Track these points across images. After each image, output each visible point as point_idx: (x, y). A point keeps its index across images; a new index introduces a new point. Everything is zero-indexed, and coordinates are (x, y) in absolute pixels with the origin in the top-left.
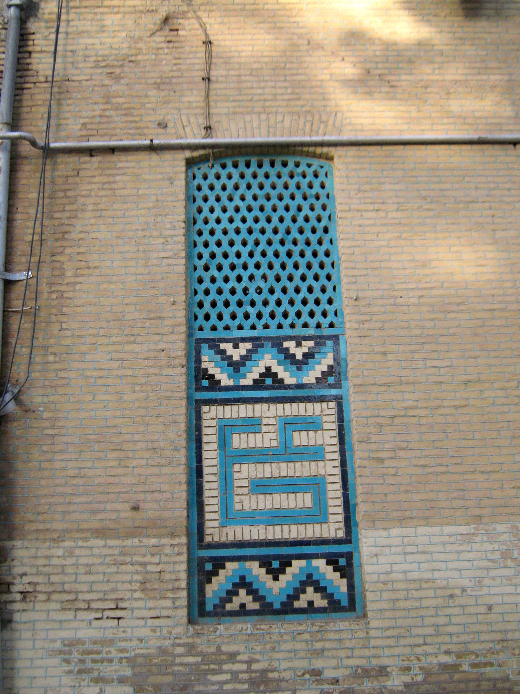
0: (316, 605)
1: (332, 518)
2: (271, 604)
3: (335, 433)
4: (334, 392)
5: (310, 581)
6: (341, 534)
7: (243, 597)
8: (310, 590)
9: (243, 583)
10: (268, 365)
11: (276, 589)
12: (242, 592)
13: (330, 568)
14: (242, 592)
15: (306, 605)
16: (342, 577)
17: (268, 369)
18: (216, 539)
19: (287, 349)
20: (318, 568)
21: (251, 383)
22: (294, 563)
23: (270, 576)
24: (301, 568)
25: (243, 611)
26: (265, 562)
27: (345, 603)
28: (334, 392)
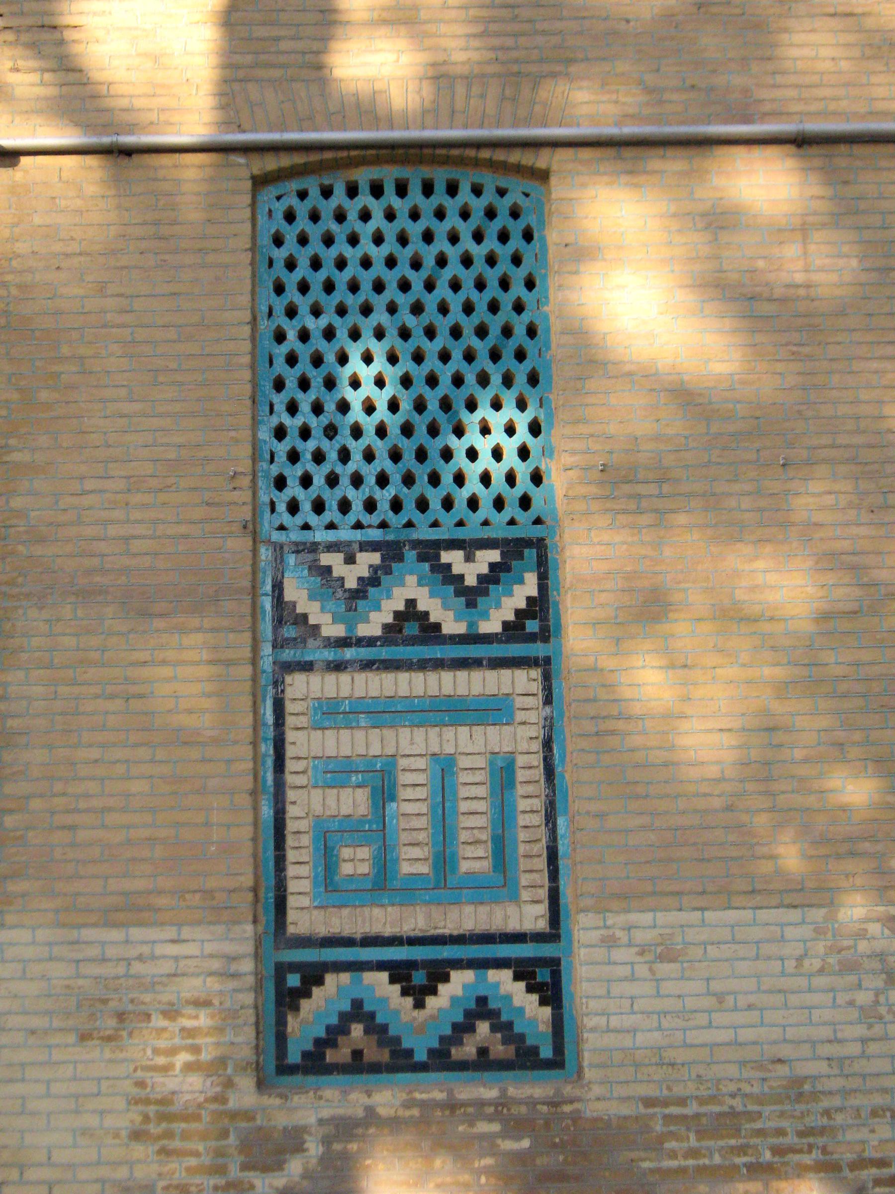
0: (492, 1056)
2: (410, 1053)
4: (538, 649)
5: (481, 1009)
10: (411, 596)
13: (522, 985)
16: (543, 1002)
17: (411, 603)
19: (449, 566)
20: (497, 985)
23: (409, 1001)
26: (399, 972)
27: (546, 1052)
28: (538, 649)
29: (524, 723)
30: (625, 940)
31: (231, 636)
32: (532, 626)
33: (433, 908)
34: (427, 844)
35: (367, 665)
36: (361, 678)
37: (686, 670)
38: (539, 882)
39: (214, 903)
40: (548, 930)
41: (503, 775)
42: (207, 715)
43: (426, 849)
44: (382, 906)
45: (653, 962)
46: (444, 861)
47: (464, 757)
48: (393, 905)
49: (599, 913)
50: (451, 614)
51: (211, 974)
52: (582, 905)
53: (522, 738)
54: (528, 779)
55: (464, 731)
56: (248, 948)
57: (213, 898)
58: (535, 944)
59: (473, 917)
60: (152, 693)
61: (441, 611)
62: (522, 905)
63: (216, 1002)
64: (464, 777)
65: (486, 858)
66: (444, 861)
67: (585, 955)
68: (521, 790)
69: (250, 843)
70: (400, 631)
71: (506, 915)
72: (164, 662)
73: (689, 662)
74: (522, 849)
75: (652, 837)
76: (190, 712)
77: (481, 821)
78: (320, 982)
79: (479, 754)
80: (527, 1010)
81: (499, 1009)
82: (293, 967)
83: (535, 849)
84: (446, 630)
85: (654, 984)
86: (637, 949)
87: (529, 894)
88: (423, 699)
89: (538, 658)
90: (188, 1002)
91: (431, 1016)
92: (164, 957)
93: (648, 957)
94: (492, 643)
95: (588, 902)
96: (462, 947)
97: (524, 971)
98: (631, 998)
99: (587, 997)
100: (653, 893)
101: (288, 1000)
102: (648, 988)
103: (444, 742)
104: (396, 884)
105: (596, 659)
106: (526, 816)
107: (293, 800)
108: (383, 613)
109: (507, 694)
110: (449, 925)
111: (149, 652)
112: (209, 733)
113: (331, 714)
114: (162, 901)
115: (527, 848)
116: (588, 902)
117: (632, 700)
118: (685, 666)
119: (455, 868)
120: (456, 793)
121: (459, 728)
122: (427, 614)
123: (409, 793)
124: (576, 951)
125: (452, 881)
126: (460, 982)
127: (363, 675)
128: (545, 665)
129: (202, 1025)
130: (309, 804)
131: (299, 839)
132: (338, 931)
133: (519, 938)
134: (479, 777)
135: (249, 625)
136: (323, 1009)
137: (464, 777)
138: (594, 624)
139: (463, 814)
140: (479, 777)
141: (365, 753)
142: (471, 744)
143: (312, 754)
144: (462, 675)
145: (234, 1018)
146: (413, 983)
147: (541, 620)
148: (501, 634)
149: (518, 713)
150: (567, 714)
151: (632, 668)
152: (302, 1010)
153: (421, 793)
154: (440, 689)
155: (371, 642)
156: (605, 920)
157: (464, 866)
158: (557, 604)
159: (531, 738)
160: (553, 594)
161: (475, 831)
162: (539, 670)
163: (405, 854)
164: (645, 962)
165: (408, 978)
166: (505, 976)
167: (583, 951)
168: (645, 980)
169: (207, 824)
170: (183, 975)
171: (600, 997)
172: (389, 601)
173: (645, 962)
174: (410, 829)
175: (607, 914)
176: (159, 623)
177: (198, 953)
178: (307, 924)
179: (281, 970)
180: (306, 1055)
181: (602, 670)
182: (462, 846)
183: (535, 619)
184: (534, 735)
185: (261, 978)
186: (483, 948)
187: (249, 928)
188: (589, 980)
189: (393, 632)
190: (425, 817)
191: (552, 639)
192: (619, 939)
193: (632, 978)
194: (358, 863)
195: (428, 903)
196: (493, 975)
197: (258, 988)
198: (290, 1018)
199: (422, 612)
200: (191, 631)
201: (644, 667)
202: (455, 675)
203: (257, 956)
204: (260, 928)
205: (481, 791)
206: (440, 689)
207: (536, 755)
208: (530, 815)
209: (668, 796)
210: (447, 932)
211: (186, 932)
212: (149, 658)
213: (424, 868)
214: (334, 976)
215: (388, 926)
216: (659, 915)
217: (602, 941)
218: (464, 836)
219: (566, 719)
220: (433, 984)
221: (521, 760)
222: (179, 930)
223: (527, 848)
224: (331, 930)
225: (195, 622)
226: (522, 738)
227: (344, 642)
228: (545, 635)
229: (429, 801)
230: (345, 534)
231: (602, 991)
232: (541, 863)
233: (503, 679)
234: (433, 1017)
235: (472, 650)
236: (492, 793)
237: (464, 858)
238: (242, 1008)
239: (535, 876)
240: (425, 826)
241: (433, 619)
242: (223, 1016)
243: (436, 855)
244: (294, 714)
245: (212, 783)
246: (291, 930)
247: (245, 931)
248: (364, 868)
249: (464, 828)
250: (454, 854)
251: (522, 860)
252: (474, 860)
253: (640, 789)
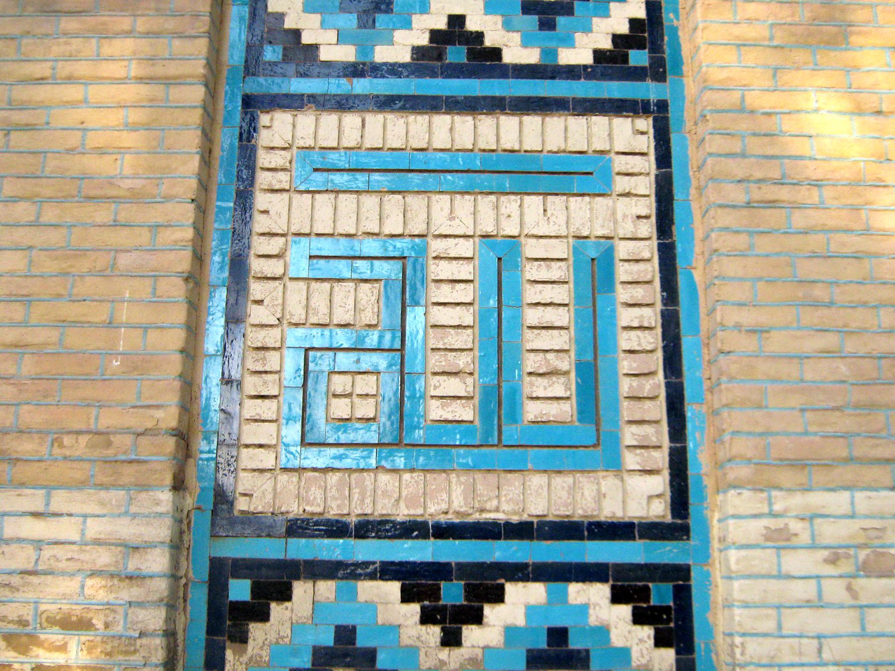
3: (648, 206)
13: (625, 611)
16: (661, 641)
20: (584, 609)
21: (406, 57)
22: (512, 590)
23: (434, 632)
24: (530, 610)
26: (418, 583)
28: (650, 91)
29: (628, 195)
30: (805, 538)
31: (177, 43)
32: (638, 58)
33: (479, 476)
34: (471, 374)
35: (386, 103)
36: (375, 120)
37: (880, 117)
38: (654, 440)
39: (110, 452)
40: (669, 519)
41: (596, 269)
42: (128, 157)
43: (470, 380)
44: (395, 471)
45: (854, 577)
46: (498, 401)
47: (533, 241)
48: (412, 470)
49: (761, 490)
50: (516, 37)
51: (93, 574)
52: (731, 476)
53: (625, 216)
54: (635, 278)
55: (533, 203)
56: (162, 531)
57: (109, 444)
58: (648, 541)
59: (545, 493)
60: (48, 123)
61: (503, 32)
62: (626, 476)
63: (98, 623)
64: (533, 272)
65: (568, 398)
66: (498, 401)
67: (738, 562)
68: (623, 294)
69: (177, 358)
70: (440, 57)
71: (599, 491)
72: (70, 79)
73: (884, 109)
74: (626, 386)
75: (843, 369)
76: (101, 151)
77: (558, 340)
78: (285, 595)
79: (557, 237)
80: (635, 654)
81: (587, 651)
83: (648, 387)
84: (508, 58)
85: (854, 614)
86: (826, 553)
87: (638, 459)
88: (472, 154)
89: (649, 101)
90: (52, 621)
91: (470, 659)
92: (19, 540)
93: (846, 567)
94: (579, 78)
95: (742, 472)
96: (525, 543)
97: (628, 587)
98: (819, 637)
99: (743, 635)
100: (850, 460)
102: (846, 621)
103: (502, 219)
104: (419, 435)
105: (743, 97)
106: (633, 334)
107: (258, 298)
108: (414, 31)
109: (602, 152)
110: (505, 507)
111: (49, 64)
112: (128, 183)
113: (327, 169)
114: (26, 447)
115: (635, 384)
116: (742, 472)
117: (801, 158)
118: (879, 113)
119: (514, 418)
120: (519, 295)
121: (527, 198)
122: (480, 36)
123: (445, 293)
124: (716, 554)
125: (511, 433)
126: (521, 601)
127: (380, 117)
128: (659, 111)
129: (70, 662)
130: (283, 304)
131: (264, 359)
132: (319, 510)
134: (556, 272)
135: (206, 28)
136: (287, 640)
137: (533, 272)
138: (739, 46)
139: (530, 328)
140: (556, 272)
141: (376, 231)
142: (544, 222)
143: (294, 229)
144: (532, 122)
145: (126, 653)
146: (441, 603)
147: (652, 51)
148: (591, 66)
149: (618, 178)
150: (694, 183)
151: (798, 111)
152: (250, 641)
153: (464, 293)
154: (498, 141)
155: (394, 70)
156: (770, 504)
157: (532, 411)
158: (675, 30)
159: (639, 217)
160: (668, 17)
161: (550, 356)
162: (650, 121)
163: (435, 387)
164: (841, 577)
165: (434, 593)
166: (597, 594)
167: (733, 555)
168: (842, 607)
169: (111, 324)
170: (45, 573)
171: (765, 635)
172: (425, 16)
173: (841, 577)
174: (446, 349)
175: (774, 493)
176: (70, 24)
177: (76, 537)
178: (269, 497)
179: (220, 572)
181: (752, 112)
182: (527, 379)
183: (644, 48)
184: (644, 213)
185: (186, 585)
186: (562, 547)
187: (165, 497)
188: (746, 605)
189: (428, 59)
190: (469, 331)
191: (669, 78)
192: (796, 535)
193: (818, 604)
194: (356, 400)
195: (468, 469)
196: (576, 592)
197: (174, 603)
198: (229, 654)
199: (471, 33)
200: (117, 35)
201: (816, 111)
202: (521, 123)
203: (177, 546)
204: (189, 502)
205: (560, 294)
206: (498, 141)
207: (647, 243)
208: (638, 333)
209: (864, 304)
210: (500, 517)
211: (60, 500)
212: (48, 73)
213: (465, 412)
214: (309, 584)
215: (402, 504)
216: (859, 496)
217: (767, 538)
218: (532, 362)
219: (693, 191)
220: (476, 604)
221: (623, 249)
222: (48, 497)
223: (635, 384)
224: (308, 508)
225: (125, 23)
226: (625, 216)
227: (355, 70)
228: (658, 71)
229: (476, 307)
231: (769, 625)
232: (658, 410)
233: (595, 129)
234: (473, 661)
235: (543, 92)
236: (578, 298)
237: (532, 398)
238: (142, 635)
239: (648, 430)
240: (470, 346)
241: (488, 43)
242: (109, 648)
243: (486, 391)
244: (269, 170)
245: (124, 261)
247: (158, 503)
249: (532, 351)
250: (515, 392)
251: (626, 403)
252: (547, 401)
253: (819, 292)
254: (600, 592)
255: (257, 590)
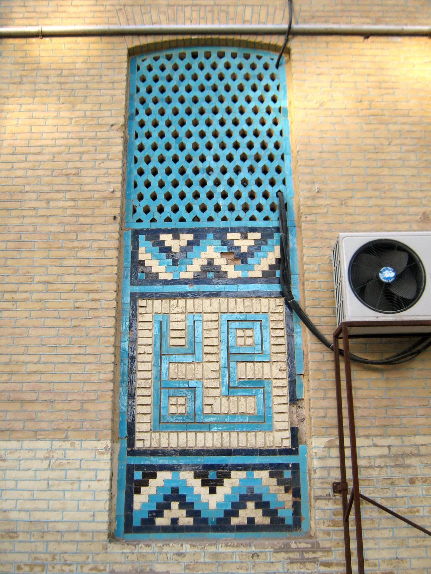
1: (278, 426)
2: (206, 520)
6: (287, 444)
7: (175, 510)
8: (251, 505)
9: (175, 495)
11: (212, 502)
12: (175, 505)
14: (175, 505)
15: (245, 522)
18: (147, 445)
25: (174, 527)
82: (139, 467)
101: (134, 487)
133: (271, 452)
180: (143, 521)
196: (257, 474)
230: (175, 224)
246: (138, 445)
248: (182, 410)
254: (265, 474)
255: (144, 475)
